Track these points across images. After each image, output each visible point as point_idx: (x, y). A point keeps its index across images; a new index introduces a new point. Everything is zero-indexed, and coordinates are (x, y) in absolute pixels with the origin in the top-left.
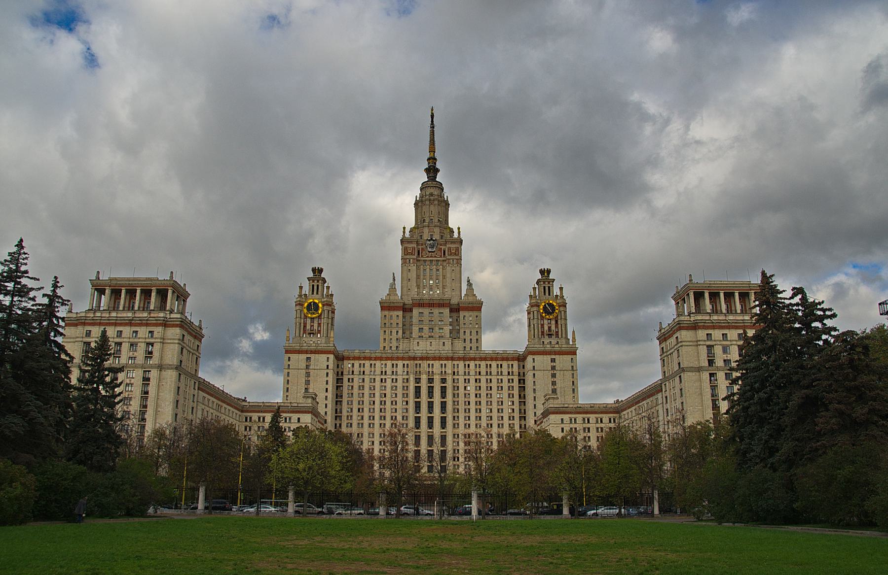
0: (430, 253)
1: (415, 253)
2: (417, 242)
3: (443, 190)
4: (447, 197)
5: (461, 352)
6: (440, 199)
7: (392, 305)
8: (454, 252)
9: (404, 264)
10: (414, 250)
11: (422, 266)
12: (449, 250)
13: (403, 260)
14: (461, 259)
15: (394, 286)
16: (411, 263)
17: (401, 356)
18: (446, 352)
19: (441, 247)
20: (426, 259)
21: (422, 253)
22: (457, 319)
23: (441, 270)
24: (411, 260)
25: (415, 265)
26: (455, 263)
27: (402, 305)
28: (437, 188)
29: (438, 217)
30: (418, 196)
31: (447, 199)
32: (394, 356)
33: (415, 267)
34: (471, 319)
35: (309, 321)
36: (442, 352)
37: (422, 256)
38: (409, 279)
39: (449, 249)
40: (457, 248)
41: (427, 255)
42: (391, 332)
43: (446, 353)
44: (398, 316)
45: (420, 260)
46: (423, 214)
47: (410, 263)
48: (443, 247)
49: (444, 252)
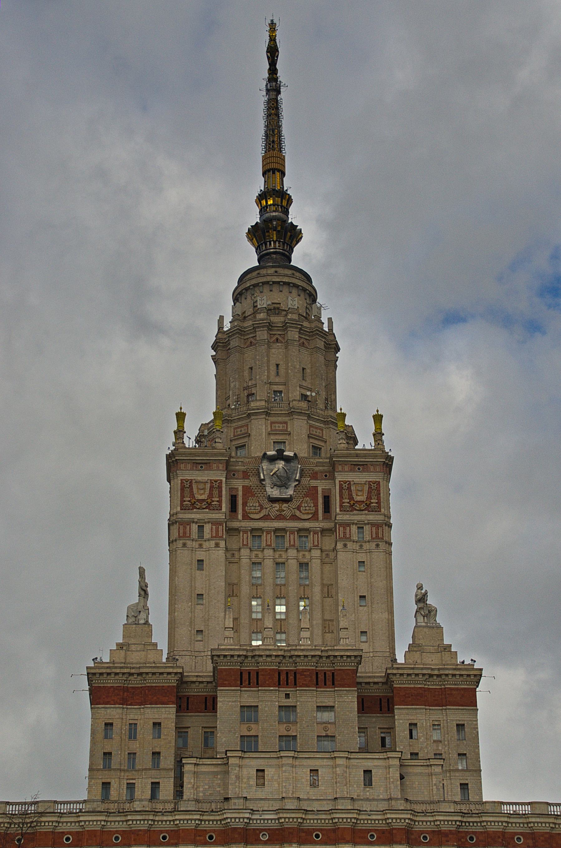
0: (277, 506)
1: (220, 502)
2: (228, 463)
3: (312, 296)
4: (330, 320)
5: (445, 807)
6: (306, 324)
7: (135, 682)
8: (363, 498)
9: (180, 543)
10: (215, 492)
11: (245, 552)
12: (346, 493)
13: (175, 527)
14: (390, 526)
15: (143, 616)
16: (207, 535)
17: (192, 825)
18: (382, 806)
19: (314, 483)
20: (260, 524)
21: (245, 504)
22: (383, 739)
23: (315, 565)
24: (207, 528)
25: (222, 544)
26: (367, 537)
27: (173, 681)
28: (295, 291)
29: (301, 387)
30: (228, 319)
31: (331, 329)
32: (158, 827)
33: (220, 553)
34: (436, 736)
36: (366, 806)
37: (246, 517)
38: (200, 596)
39: (346, 487)
40: (374, 486)
41: (262, 515)
42: (131, 787)
43: (383, 812)
44: (157, 725)
45: (237, 530)
46: (246, 374)
48: (321, 485)
49: (327, 500)
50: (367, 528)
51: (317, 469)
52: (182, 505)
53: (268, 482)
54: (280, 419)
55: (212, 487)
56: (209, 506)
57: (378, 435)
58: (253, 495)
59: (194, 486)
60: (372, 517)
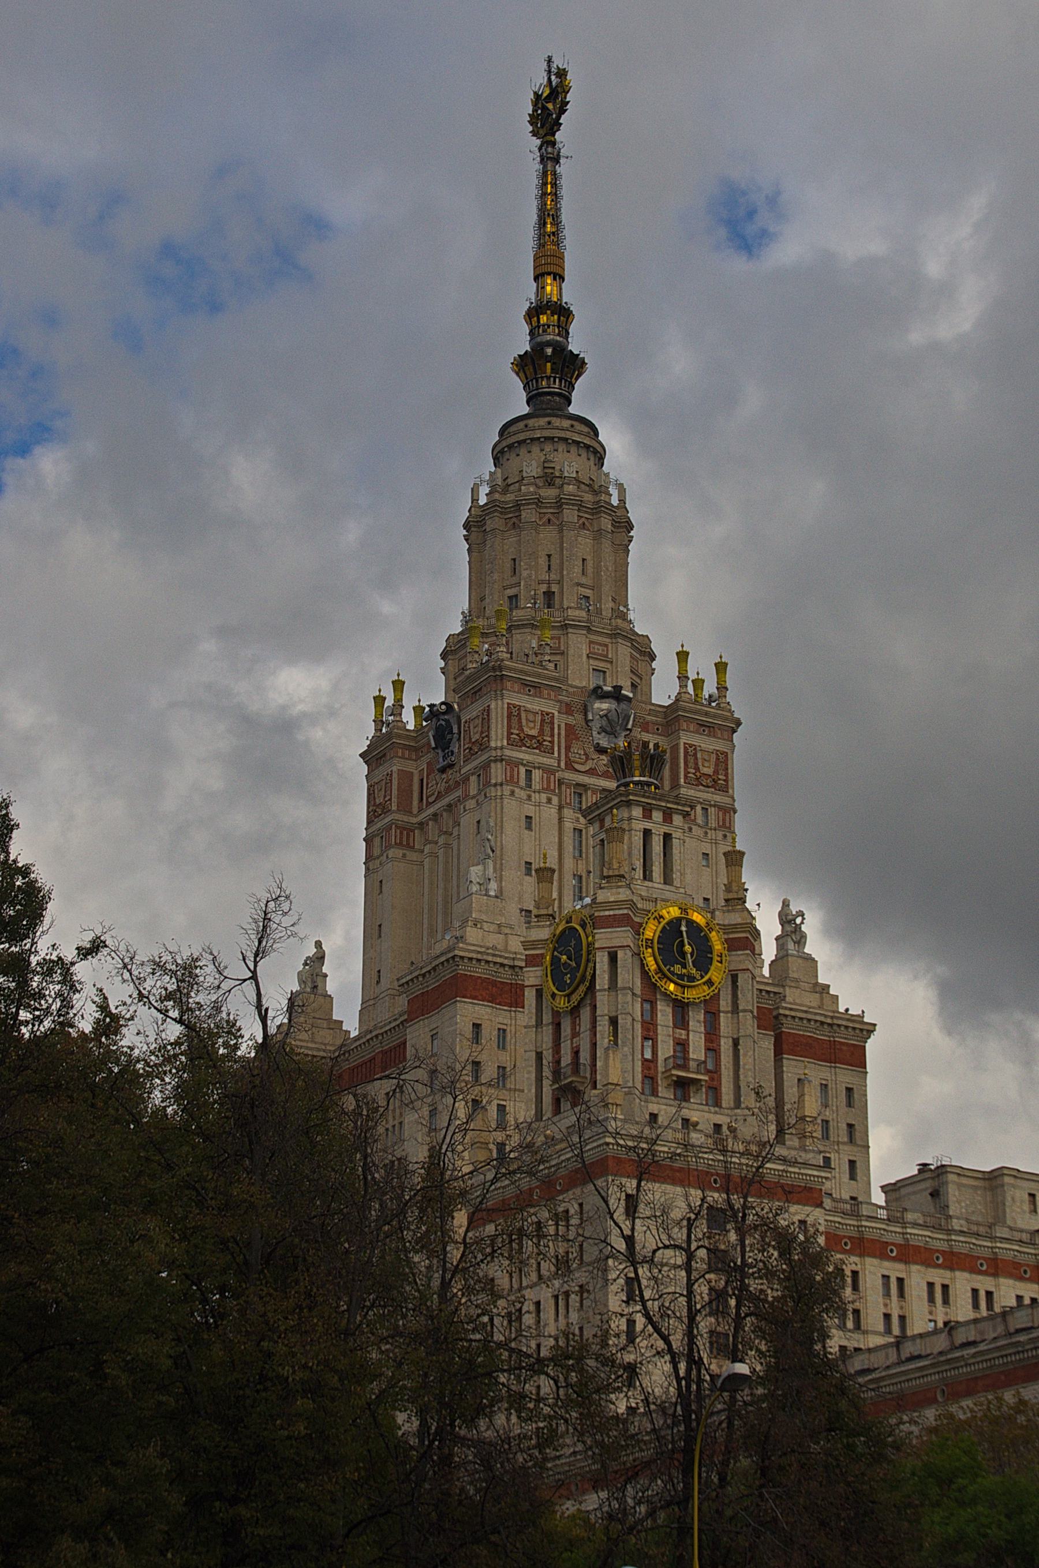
8: (709, 771)
10: (547, 729)
12: (691, 759)
16: (536, 785)
24: (536, 774)
25: (555, 800)
35: (665, 1014)
39: (692, 752)
47: (529, 786)
50: (712, 811)
51: (649, 718)
52: (509, 739)
53: (596, 726)
54: (600, 639)
55: (543, 721)
56: (540, 745)
57: (722, 688)
58: (577, 739)
59: (523, 715)
60: (718, 798)
